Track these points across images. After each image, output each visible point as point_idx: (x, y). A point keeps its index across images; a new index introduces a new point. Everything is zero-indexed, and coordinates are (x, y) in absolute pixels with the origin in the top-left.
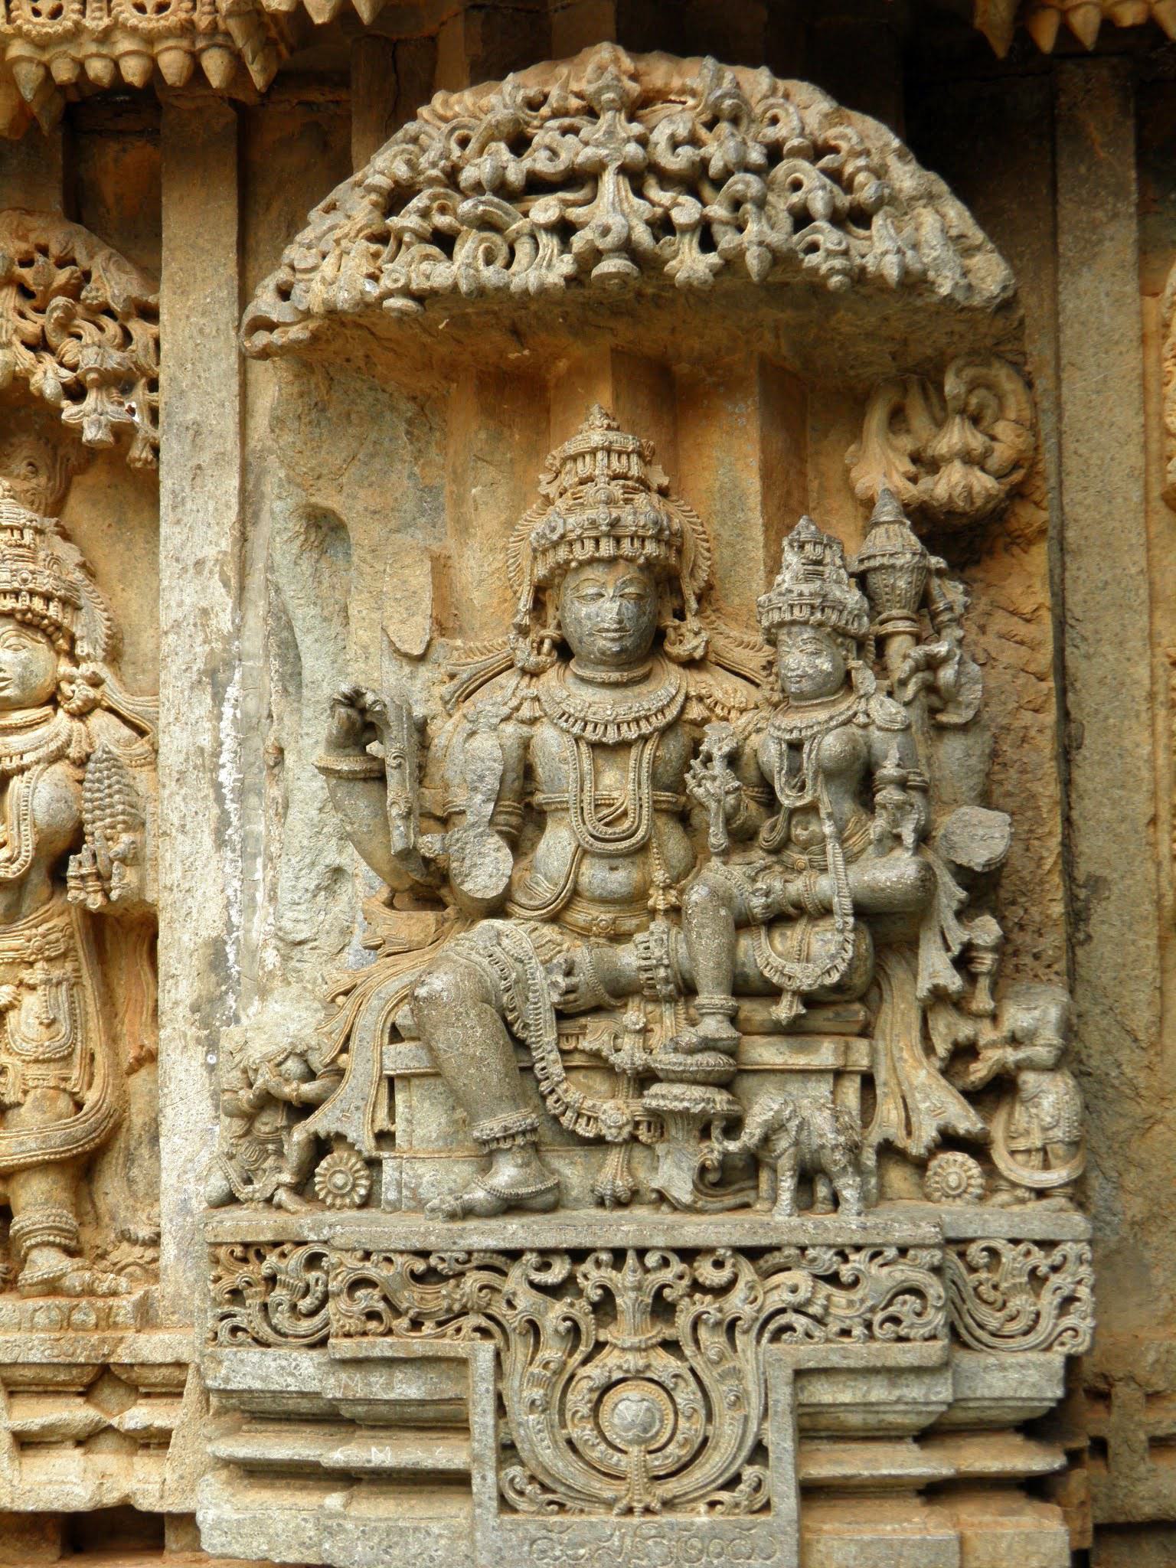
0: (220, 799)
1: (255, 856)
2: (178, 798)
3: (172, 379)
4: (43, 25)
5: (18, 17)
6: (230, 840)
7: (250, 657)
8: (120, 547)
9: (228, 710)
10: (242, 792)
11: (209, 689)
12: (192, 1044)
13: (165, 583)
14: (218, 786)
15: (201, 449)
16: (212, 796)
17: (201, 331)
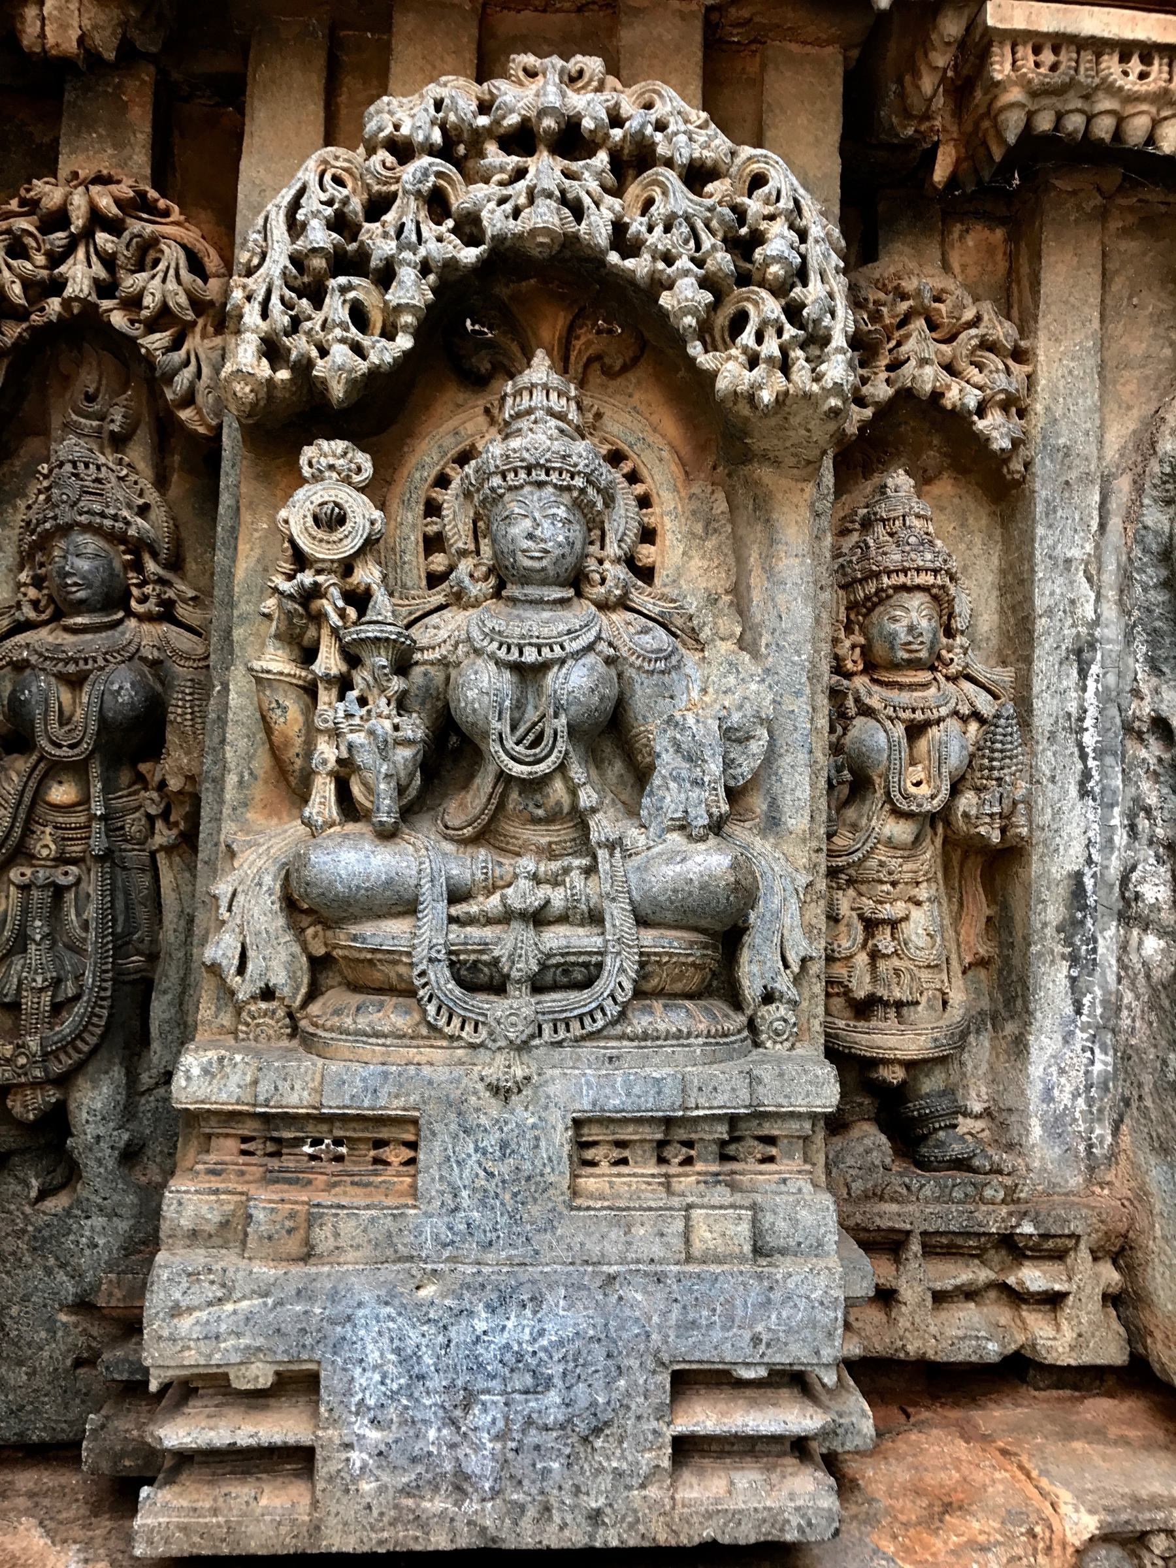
0: (1083, 757)
1: (1112, 806)
2: (1049, 754)
3: (1048, 409)
4: (1046, 76)
5: (1023, 66)
6: (1092, 791)
7: (1109, 641)
8: (962, 547)
9: (1091, 684)
10: (1100, 753)
11: (1075, 665)
12: (1058, 958)
13: (1041, 575)
14: (1081, 746)
15: (1069, 468)
16: (1077, 754)
17: (1070, 372)
